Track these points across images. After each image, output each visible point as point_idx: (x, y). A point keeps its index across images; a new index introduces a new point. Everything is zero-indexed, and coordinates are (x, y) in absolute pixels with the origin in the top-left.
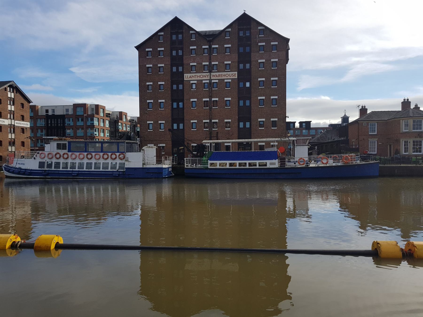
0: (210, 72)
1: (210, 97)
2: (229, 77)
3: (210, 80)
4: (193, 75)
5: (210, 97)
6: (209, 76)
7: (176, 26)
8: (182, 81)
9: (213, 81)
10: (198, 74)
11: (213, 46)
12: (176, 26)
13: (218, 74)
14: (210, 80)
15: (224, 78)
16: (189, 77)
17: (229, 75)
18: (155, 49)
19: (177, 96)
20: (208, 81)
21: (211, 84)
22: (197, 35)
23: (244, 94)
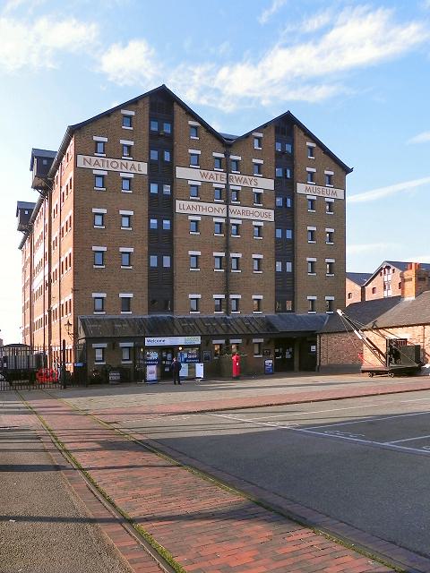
0: (227, 203)
1: (227, 249)
2: (259, 218)
3: (227, 218)
4: (195, 204)
5: (227, 249)
6: (225, 211)
7: (162, 102)
8: (169, 212)
9: (232, 221)
10: (204, 205)
11: (232, 157)
12: (162, 102)
13: (241, 208)
14: (227, 218)
15: (251, 217)
16: (186, 207)
17: (260, 214)
18: (114, 138)
19: (162, 242)
20: (223, 221)
21: (225, 227)
22: (203, 131)
23: (286, 250)
